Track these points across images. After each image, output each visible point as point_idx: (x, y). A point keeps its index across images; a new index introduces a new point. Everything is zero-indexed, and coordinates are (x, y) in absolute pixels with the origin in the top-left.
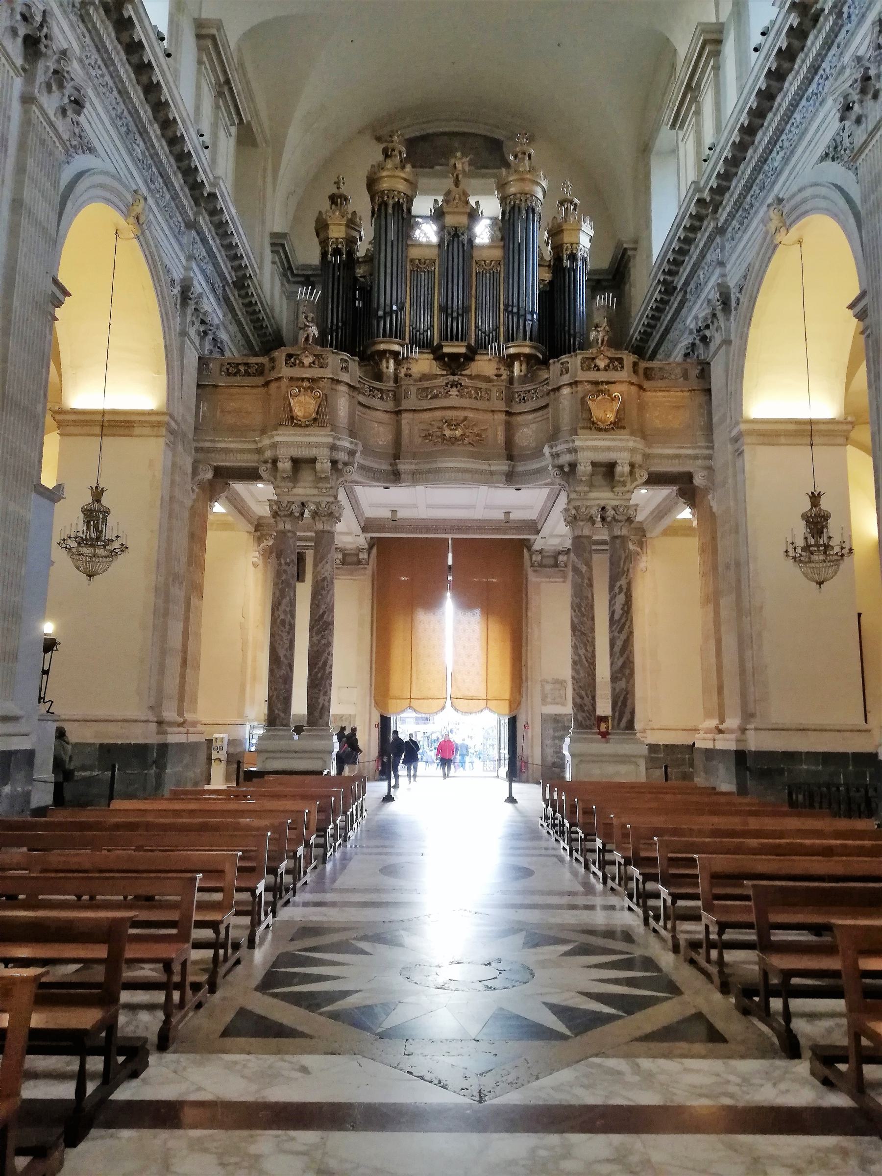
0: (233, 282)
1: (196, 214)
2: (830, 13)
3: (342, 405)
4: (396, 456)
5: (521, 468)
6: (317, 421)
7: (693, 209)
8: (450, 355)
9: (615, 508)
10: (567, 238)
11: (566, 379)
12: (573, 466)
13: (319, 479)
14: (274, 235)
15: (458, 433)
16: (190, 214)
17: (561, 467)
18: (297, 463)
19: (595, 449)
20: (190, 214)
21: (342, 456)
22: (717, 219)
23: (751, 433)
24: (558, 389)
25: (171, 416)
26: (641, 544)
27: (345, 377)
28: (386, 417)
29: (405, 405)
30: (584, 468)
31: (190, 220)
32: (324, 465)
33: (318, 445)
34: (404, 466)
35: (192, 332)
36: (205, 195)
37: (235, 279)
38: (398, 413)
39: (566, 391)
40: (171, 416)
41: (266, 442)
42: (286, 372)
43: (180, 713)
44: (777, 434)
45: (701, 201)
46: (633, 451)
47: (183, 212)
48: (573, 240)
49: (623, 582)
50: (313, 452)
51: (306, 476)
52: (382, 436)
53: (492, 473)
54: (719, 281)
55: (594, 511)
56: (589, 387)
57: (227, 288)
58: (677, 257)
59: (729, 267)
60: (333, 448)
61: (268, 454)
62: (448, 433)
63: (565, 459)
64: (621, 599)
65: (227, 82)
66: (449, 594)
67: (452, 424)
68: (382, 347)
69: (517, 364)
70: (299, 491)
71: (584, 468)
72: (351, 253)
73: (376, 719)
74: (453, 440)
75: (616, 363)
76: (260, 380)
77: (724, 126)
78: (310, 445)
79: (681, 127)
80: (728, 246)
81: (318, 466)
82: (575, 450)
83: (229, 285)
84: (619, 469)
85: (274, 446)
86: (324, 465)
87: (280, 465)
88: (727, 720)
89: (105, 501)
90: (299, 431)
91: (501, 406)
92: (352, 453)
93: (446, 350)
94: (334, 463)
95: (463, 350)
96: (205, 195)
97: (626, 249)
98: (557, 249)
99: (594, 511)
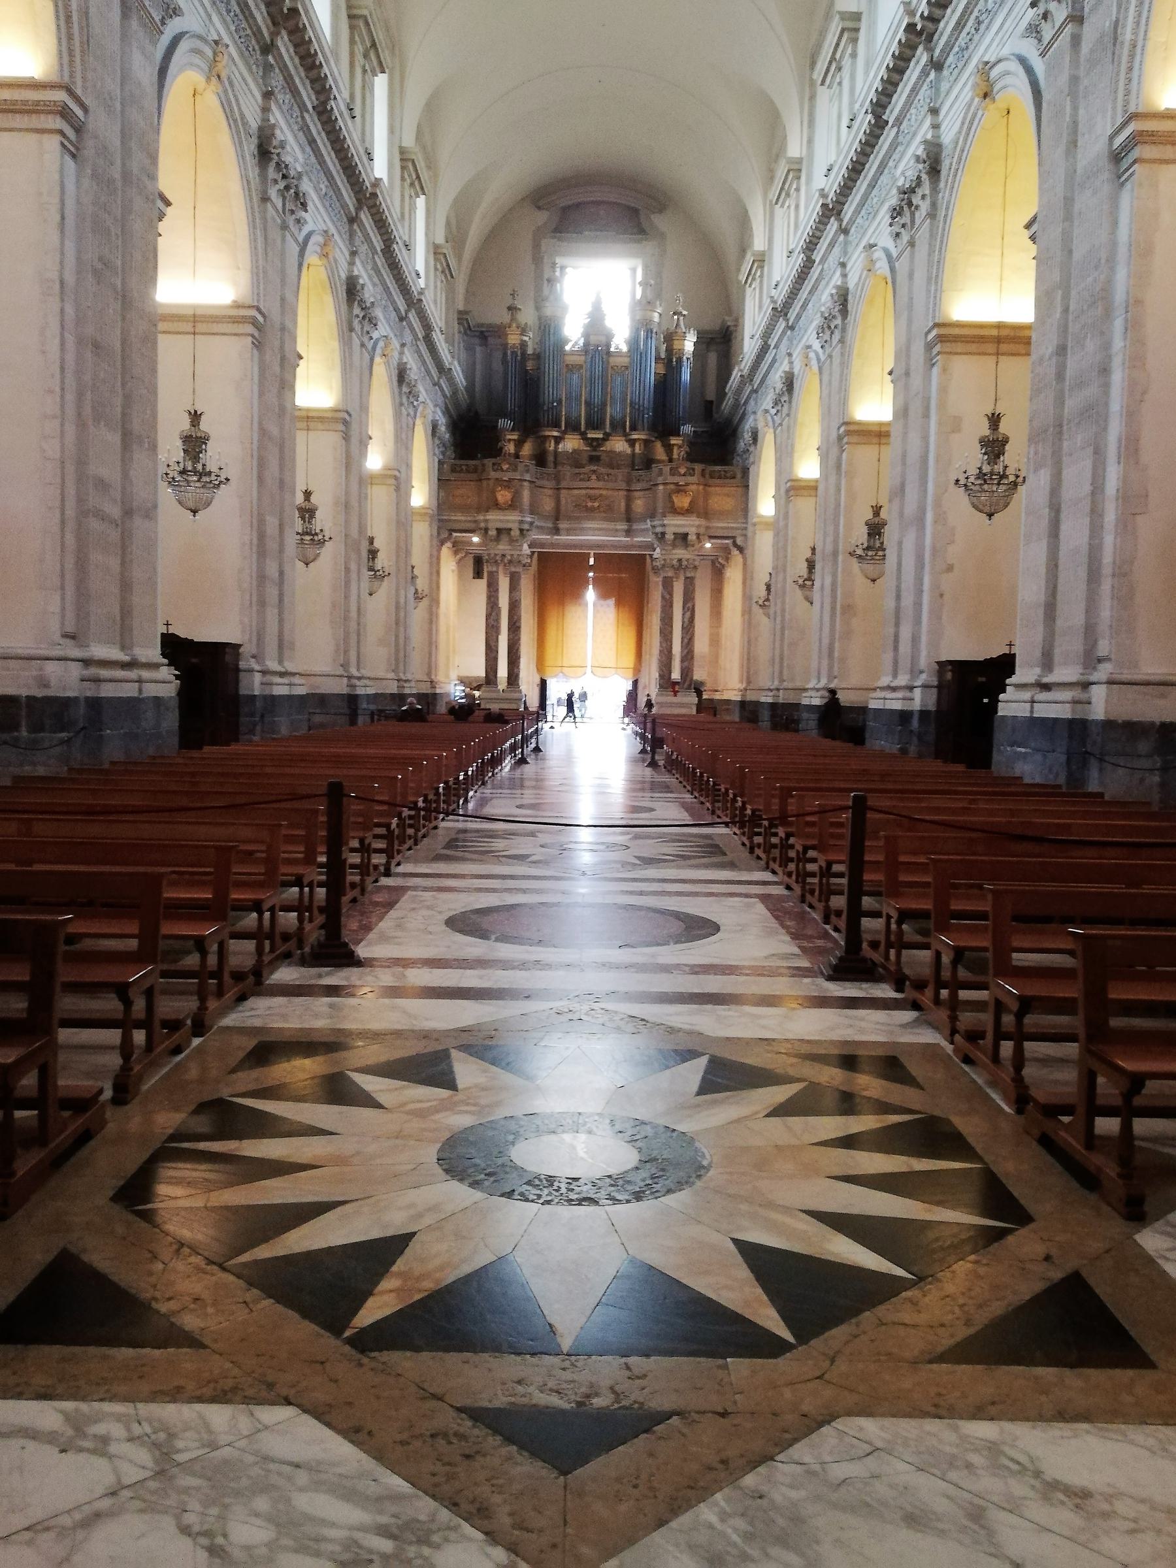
0: (314, 108)
1: (439, 378)
3: (526, 494)
4: (557, 519)
5: (635, 527)
6: (513, 505)
7: (901, 35)
8: (593, 439)
9: (688, 560)
11: (660, 480)
12: (663, 534)
13: (512, 541)
14: (460, 312)
15: (596, 504)
16: (266, 35)
17: (656, 534)
18: (499, 531)
19: (676, 526)
20: (266, 35)
21: (526, 527)
22: (842, 220)
23: (760, 523)
25: (258, 309)
26: (727, 559)
27: (527, 477)
28: (550, 492)
29: (563, 484)
30: (669, 537)
31: (265, 44)
32: (515, 533)
33: (514, 521)
34: (563, 525)
35: (273, 193)
36: (285, 11)
37: (316, 103)
38: (558, 489)
39: (661, 487)
40: (258, 309)
42: (493, 475)
43: (280, 662)
44: (981, 339)
45: (911, 27)
46: (699, 526)
47: (396, 310)
49: (690, 605)
50: (509, 526)
51: (504, 538)
52: (548, 505)
53: (617, 530)
54: (929, 136)
55: (675, 562)
56: (672, 487)
57: (306, 115)
58: (899, 62)
59: (943, 113)
60: (521, 522)
61: (482, 525)
62: (589, 504)
63: (659, 530)
64: (688, 614)
66: (591, 587)
67: (592, 498)
68: (547, 433)
69: (637, 446)
70: (500, 547)
71: (669, 537)
72: (524, 353)
73: (538, 681)
74: (592, 510)
75: (691, 472)
76: (474, 476)
78: (508, 521)
80: (944, 86)
81: (512, 533)
82: (664, 525)
83: (307, 111)
84: (689, 537)
85: (486, 521)
86: (515, 533)
87: (490, 533)
88: (899, 677)
89: (204, 425)
90: (498, 512)
91: (624, 486)
92: (531, 524)
93: (589, 436)
94: (521, 530)
95: (601, 436)
96: (285, 11)
97: (728, 327)
98: (669, 351)
99: (675, 562)
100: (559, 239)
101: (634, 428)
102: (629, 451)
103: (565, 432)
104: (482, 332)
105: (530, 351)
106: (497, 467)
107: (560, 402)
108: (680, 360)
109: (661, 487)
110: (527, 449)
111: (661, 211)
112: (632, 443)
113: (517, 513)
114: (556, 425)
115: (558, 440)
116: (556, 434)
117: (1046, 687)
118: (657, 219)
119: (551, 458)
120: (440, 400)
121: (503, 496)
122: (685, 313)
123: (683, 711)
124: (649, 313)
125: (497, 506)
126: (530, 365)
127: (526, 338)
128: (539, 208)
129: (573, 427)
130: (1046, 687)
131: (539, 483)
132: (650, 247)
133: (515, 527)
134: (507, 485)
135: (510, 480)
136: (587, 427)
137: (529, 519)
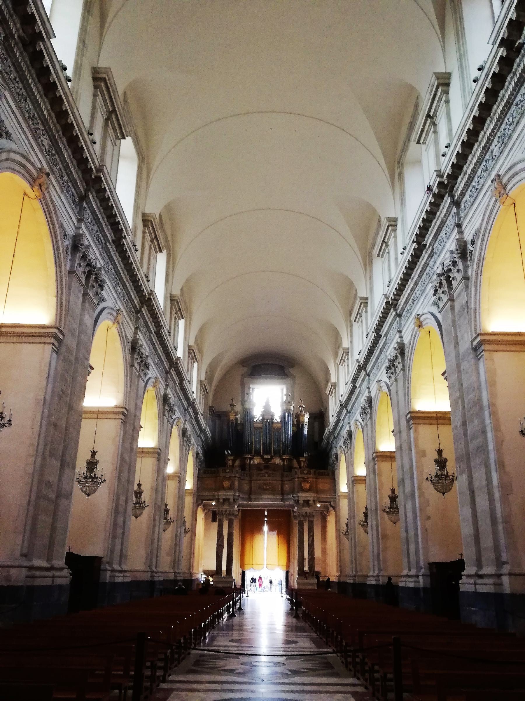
2: (429, 247)
3: (236, 483)
5: (285, 497)
6: (231, 488)
7: (384, 305)
9: (309, 513)
10: (301, 419)
11: (296, 476)
12: (298, 501)
13: (230, 504)
14: (210, 407)
17: (295, 501)
18: (224, 500)
19: (303, 497)
20: (138, 307)
21: (237, 497)
22: (367, 371)
23: (342, 496)
24: (294, 478)
25: (125, 408)
26: (328, 512)
27: (237, 475)
28: (246, 482)
29: (254, 478)
30: (301, 502)
31: (138, 310)
32: (231, 500)
34: (253, 497)
36: (146, 299)
37: (156, 330)
38: (251, 481)
39: (296, 479)
40: (125, 408)
41: (216, 494)
43: (120, 565)
44: (430, 418)
45: (387, 303)
46: (314, 497)
47: (183, 407)
48: (303, 420)
49: (311, 534)
50: (229, 497)
51: (226, 503)
52: (246, 488)
53: (277, 499)
54: (399, 341)
55: (304, 514)
56: (302, 479)
59: (403, 332)
60: (234, 496)
61: (216, 497)
62: (265, 487)
63: (296, 499)
64: (311, 538)
65: (156, 237)
66: (266, 525)
67: (265, 485)
68: (246, 456)
69: (285, 461)
71: (301, 502)
72: (236, 423)
73: (241, 571)
74: (266, 489)
75: (309, 473)
77: (399, 263)
79: (382, 256)
80: (403, 323)
82: (298, 497)
83: (152, 333)
84: (310, 502)
85: (218, 495)
86: (231, 500)
91: (280, 479)
92: (239, 496)
93: (264, 457)
94: (234, 500)
95: (270, 457)
96: (146, 299)
98: (298, 421)
99: (304, 514)
100: (252, 378)
101: (284, 453)
102: (282, 463)
103: (254, 456)
104: (219, 415)
105: (239, 422)
106: (224, 471)
107: (252, 443)
108: (303, 425)
109: (296, 479)
110: (237, 463)
111: (293, 366)
112: (283, 460)
113: (232, 491)
114: (250, 453)
115: (251, 459)
116: (250, 456)
117: (481, 577)
118: (292, 371)
119: (247, 467)
120: (200, 442)
121: (226, 484)
122: (304, 406)
123: (310, 587)
124: (289, 406)
125: (224, 489)
126: (239, 428)
127: (238, 417)
128: (243, 366)
129: (257, 453)
130: (481, 577)
131: (242, 478)
132: (289, 381)
133: (231, 498)
134: (229, 479)
135: (230, 477)
136: (263, 453)
137: (237, 494)
